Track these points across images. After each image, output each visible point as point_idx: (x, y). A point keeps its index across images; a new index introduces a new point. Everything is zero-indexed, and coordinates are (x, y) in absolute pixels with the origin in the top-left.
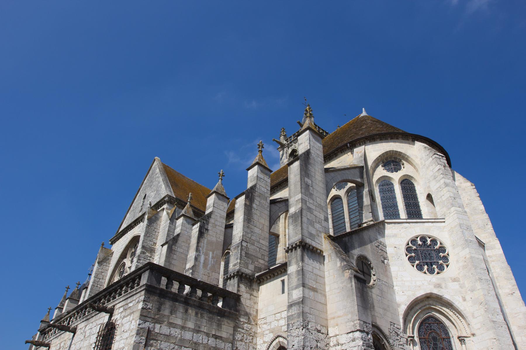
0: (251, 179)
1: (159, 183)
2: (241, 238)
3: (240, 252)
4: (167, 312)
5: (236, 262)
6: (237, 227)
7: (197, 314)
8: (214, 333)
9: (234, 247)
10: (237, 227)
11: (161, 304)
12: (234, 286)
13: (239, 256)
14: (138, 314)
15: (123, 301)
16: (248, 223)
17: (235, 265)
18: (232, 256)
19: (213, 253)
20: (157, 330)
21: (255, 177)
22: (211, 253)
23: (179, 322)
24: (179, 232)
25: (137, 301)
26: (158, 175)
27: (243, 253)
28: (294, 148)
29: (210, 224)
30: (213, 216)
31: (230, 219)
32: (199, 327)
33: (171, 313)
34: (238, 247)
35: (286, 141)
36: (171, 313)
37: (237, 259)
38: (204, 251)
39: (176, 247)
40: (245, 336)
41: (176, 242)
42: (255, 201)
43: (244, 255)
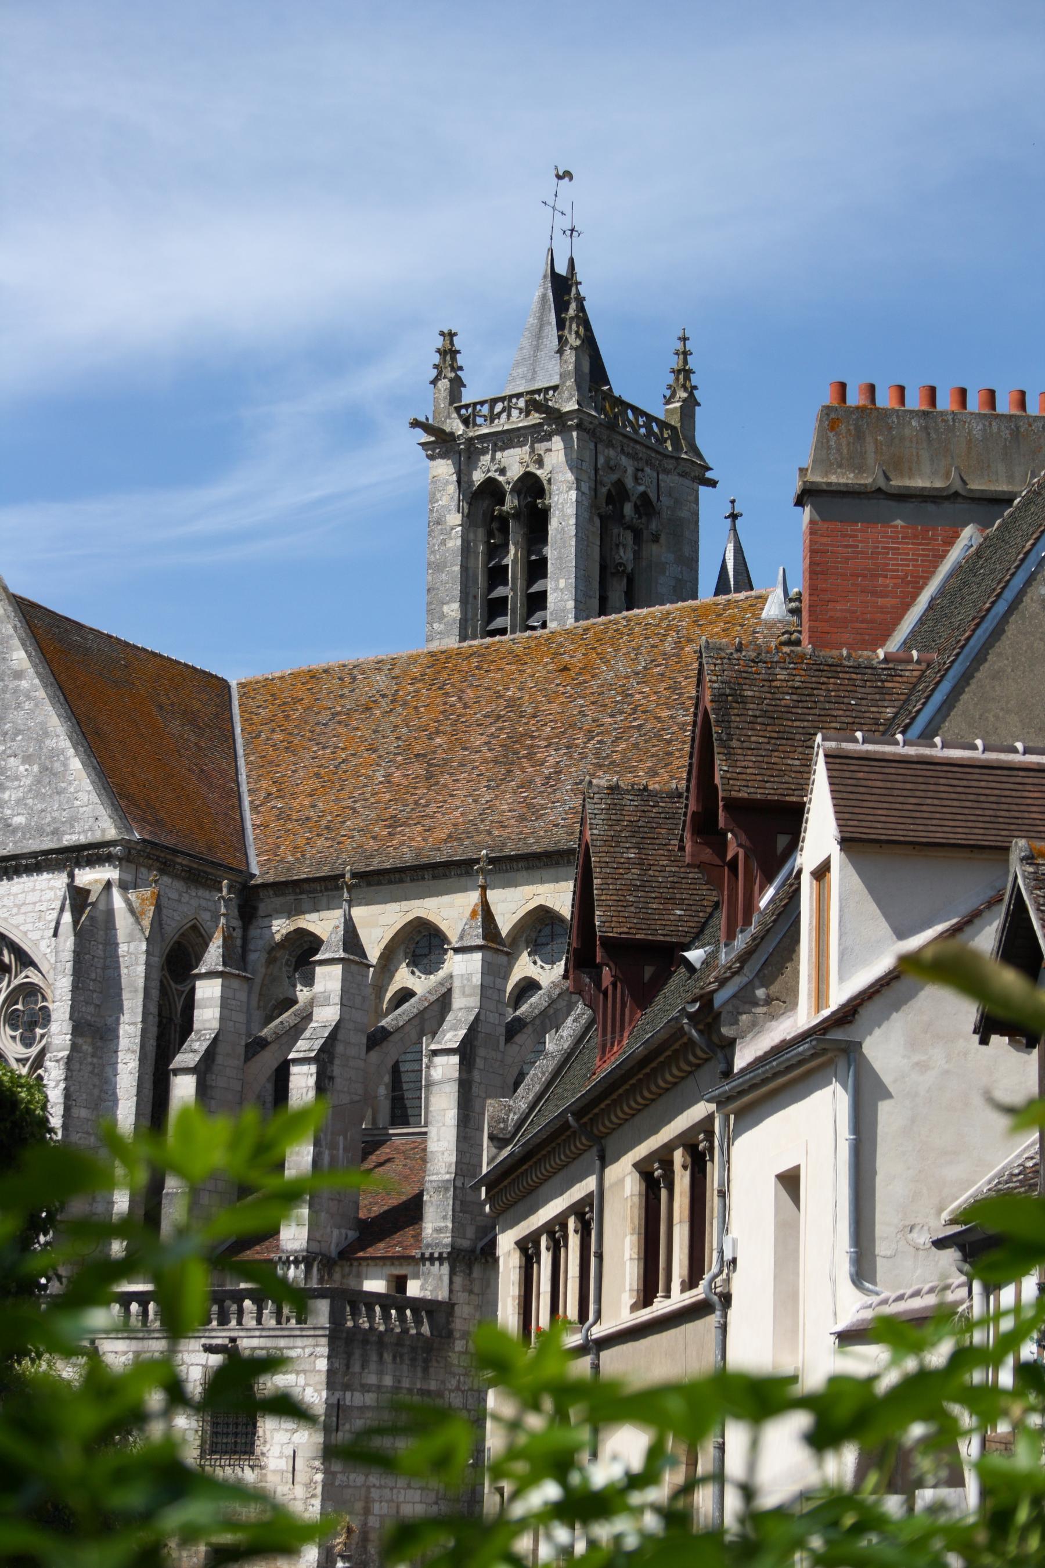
0: (464, 987)
1: (46, 734)
2: (453, 1169)
3: (451, 1203)
4: (356, 1368)
5: (443, 1225)
6: (438, 1134)
7: (394, 1358)
8: (419, 1386)
9: (435, 1185)
10: (438, 1134)
11: (349, 1355)
12: (440, 1278)
13: (450, 1213)
14: (323, 1378)
15: (260, 1337)
16: (465, 1127)
17: (439, 1230)
18: (428, 1204)
19: (345, 1138)
20: (348, 1403)
21: (475, 986)
22: (341, 1138)
23: (372, 1379)
24: (216, 1025)
25: (308, 1351)
26: (24, 684)
27: (458, 1203)
28: (496, 476)
29: (337, 1062)
30: (340, 1036)
31: (301, 893)
32: (399, 1382)
33: (363, 1367)
34: (447, 1189)
35: (458, 410)
36: (363, 1367)
37: (444, 1218)
38: (329, 1137)
39: (214, 1077)
40: (462, 1378)
41: (213, 1061)
42: (478, 1060)
43: (458, 1209)
